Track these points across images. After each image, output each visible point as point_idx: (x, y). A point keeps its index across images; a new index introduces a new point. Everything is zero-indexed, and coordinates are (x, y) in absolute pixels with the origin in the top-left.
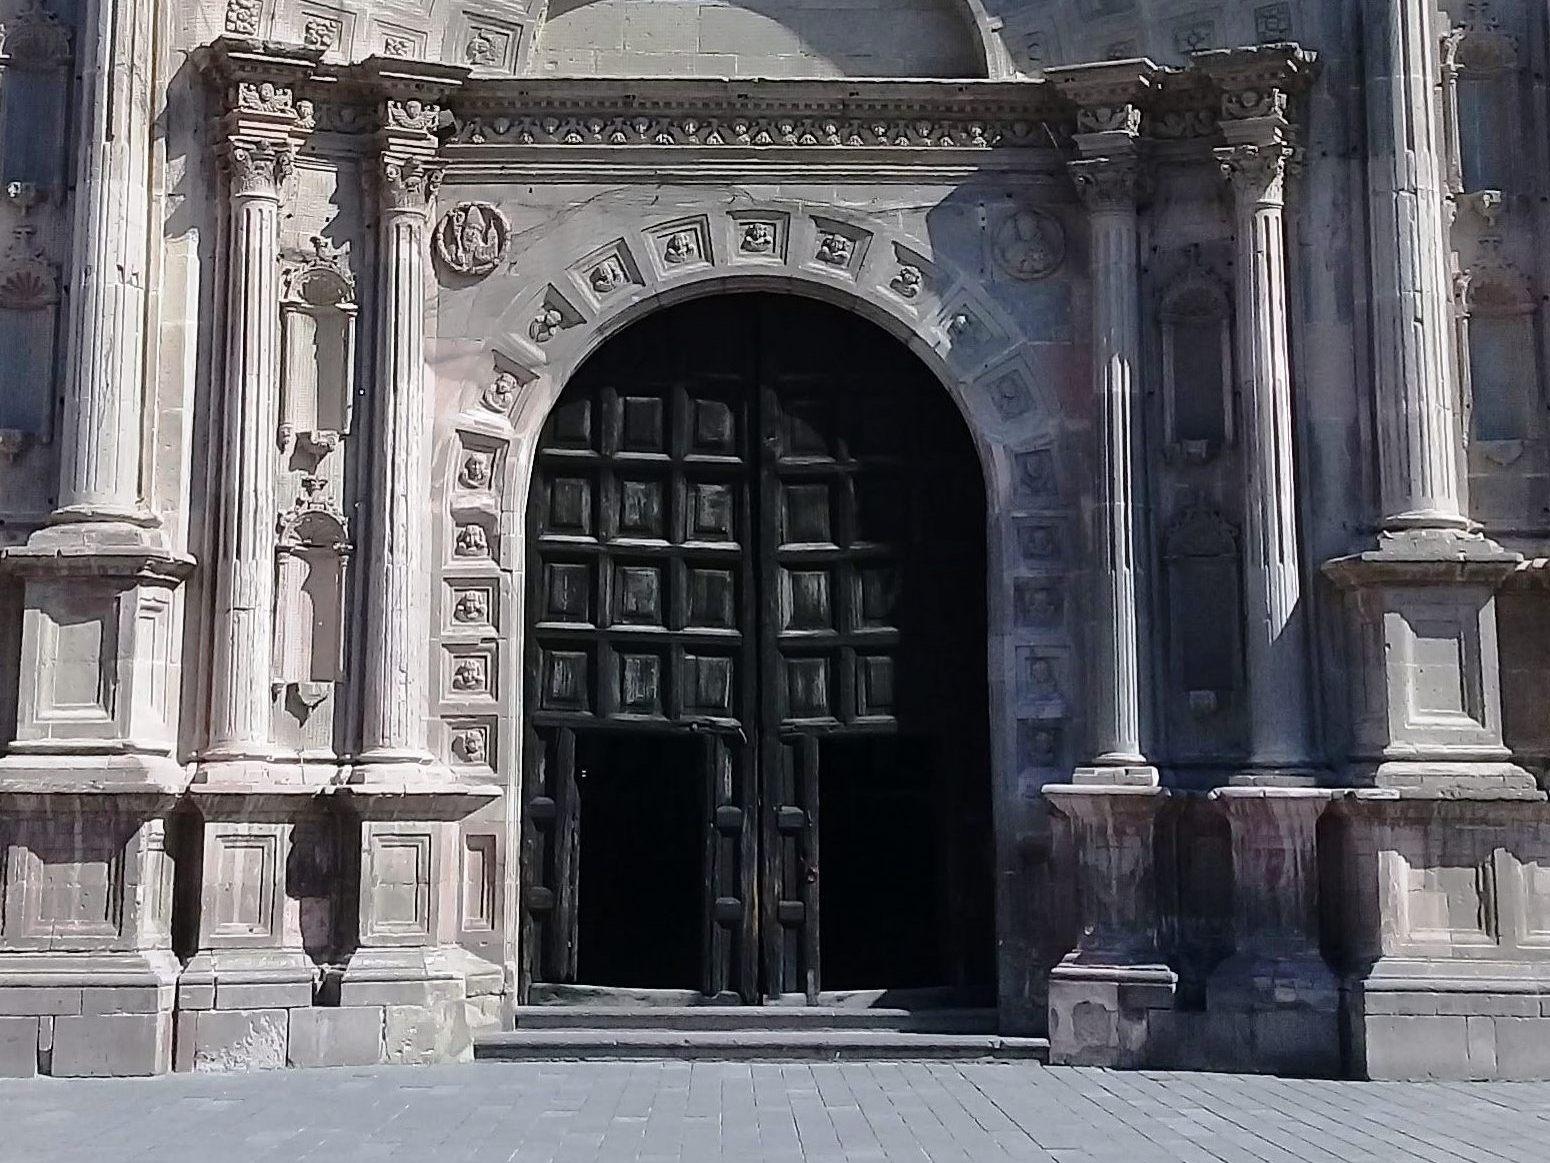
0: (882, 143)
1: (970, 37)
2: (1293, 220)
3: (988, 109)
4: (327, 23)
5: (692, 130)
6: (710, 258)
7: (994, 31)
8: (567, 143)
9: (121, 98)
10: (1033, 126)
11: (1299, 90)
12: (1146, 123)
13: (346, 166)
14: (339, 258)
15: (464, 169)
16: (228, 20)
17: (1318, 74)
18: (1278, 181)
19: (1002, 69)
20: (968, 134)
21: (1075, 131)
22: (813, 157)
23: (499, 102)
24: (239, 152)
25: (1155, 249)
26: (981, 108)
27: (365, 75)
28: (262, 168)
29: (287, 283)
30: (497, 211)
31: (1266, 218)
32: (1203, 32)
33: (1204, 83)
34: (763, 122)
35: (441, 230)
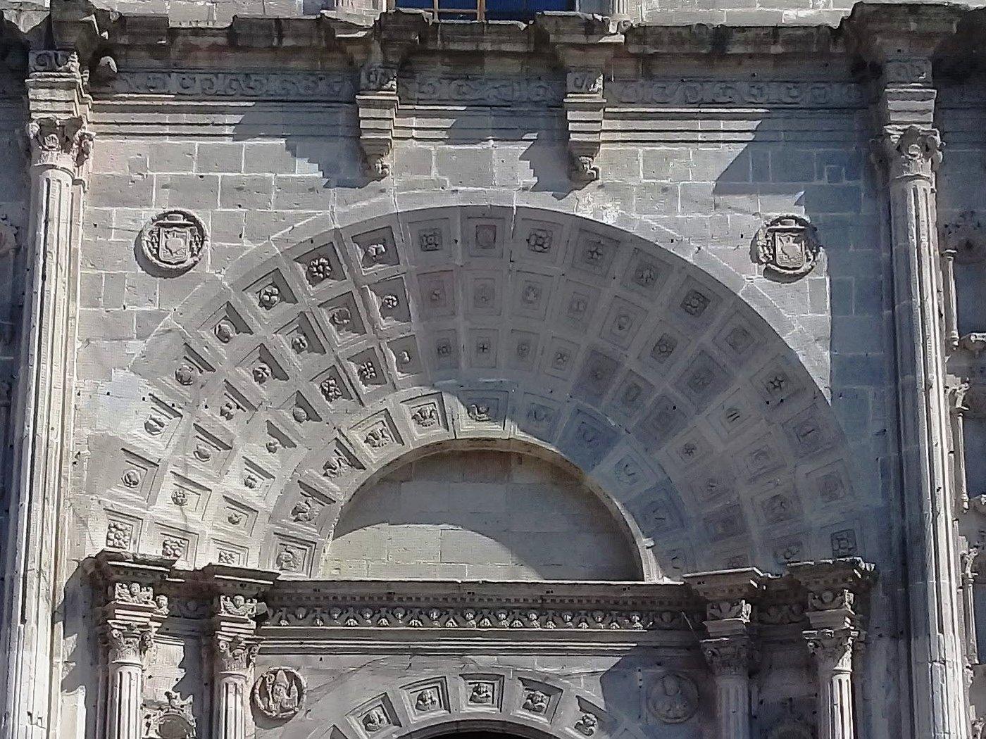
0: (570, 627)
1: (631, 552)
2: (858, 682)
3: (643, 603)
4: (178, 541)
5: (435, 617)
6: (447, 708)
7: (648, 548)
8: (347, 626)
9: (32, 593)
10: (674, 615)
11: (862, 590)
12: (755, 614)
13: (192, 642)
14: (185, 706)
15: (271, 644)
16: (108, 538)
17: (876, 580)
18: (848, 654)
19: (654, 575)
20: (630, 621)
21: (706, 620)
22: (518, 636)
23: (299, 597)
24: (115, 632)
25: (761, 702)
26: (639, 602)
27: (205, 578)
28: (130, 643)
29: (148, 725)
30: (297, 673)
31: (840, 681)
32: (794, 549)
33: (795, 585)
34: (485, 611)
35: (258, 687)
